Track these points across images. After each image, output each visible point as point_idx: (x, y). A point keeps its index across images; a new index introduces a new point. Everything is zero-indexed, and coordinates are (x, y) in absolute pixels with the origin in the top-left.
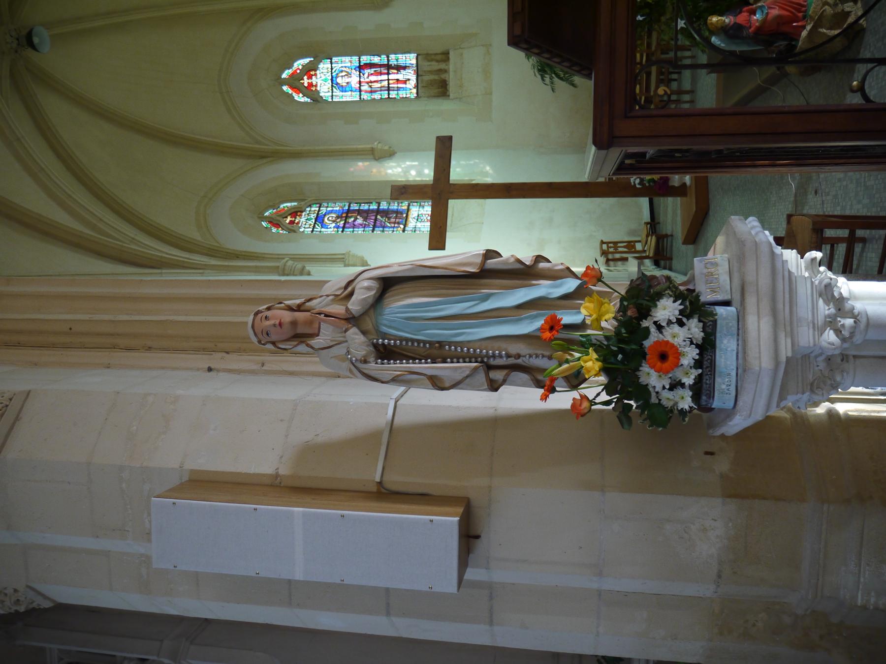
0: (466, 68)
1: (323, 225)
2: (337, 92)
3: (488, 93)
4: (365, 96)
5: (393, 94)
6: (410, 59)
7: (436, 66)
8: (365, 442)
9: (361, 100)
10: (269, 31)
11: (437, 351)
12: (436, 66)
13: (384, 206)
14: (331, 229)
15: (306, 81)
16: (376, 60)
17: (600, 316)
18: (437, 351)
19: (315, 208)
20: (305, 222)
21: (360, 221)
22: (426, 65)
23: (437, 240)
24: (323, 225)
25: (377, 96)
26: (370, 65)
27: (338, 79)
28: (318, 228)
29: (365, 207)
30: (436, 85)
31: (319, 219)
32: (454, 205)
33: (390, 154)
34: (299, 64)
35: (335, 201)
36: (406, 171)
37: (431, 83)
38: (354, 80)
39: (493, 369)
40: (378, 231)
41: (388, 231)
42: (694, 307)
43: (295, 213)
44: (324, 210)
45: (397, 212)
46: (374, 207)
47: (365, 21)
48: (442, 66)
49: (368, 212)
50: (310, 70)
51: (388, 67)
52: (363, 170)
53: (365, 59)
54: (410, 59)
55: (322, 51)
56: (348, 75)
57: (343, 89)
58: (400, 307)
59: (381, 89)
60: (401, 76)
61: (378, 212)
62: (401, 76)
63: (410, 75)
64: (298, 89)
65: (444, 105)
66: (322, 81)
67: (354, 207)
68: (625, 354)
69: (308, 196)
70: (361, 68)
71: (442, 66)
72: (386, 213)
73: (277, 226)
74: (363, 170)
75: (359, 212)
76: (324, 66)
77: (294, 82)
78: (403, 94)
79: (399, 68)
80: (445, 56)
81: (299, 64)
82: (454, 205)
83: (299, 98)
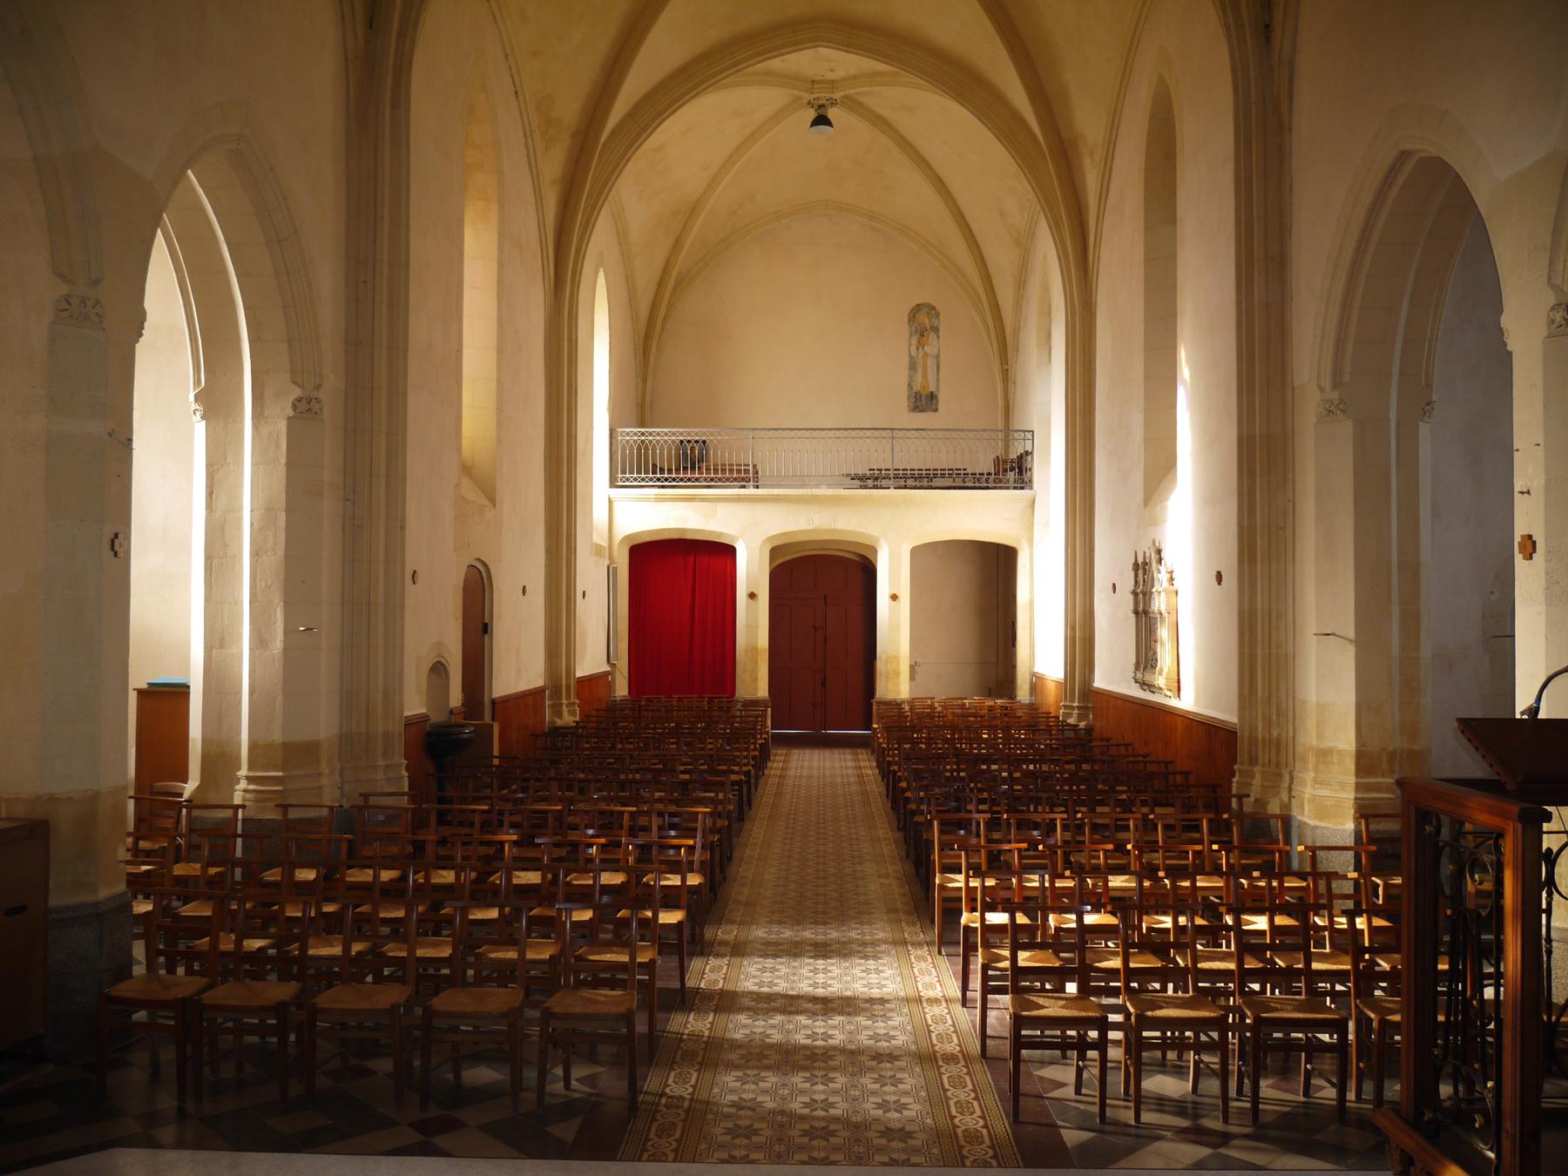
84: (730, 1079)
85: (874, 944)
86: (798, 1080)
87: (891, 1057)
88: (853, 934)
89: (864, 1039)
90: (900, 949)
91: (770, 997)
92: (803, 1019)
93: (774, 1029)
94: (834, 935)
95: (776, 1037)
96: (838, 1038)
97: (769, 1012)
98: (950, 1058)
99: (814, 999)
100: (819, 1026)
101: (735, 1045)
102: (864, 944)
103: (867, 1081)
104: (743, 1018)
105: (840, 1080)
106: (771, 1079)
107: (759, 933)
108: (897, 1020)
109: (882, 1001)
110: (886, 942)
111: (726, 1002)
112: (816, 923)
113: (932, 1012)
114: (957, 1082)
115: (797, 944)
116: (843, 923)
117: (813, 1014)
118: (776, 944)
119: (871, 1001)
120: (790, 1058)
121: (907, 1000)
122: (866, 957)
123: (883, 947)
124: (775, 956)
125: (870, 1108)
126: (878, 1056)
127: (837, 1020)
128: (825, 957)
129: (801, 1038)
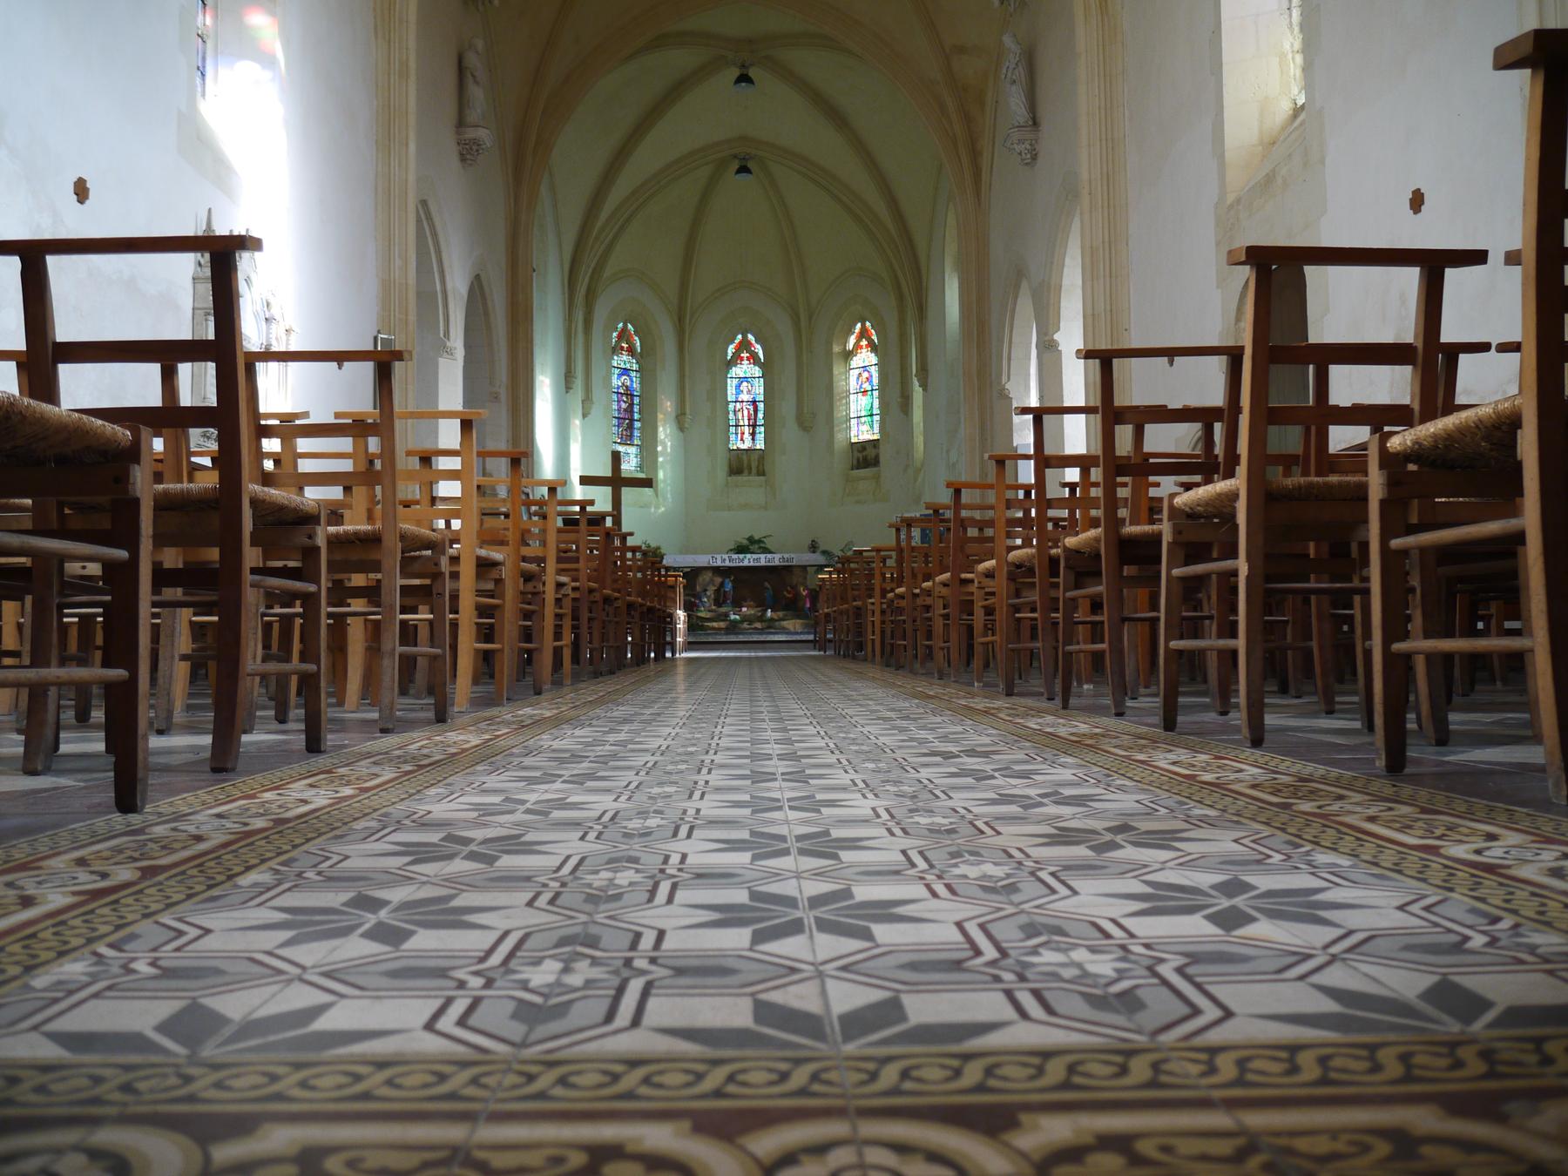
0: (751, 489)
1: (620, 375)
2: (735, 382)
3: (729, 509)
4: (731, 406)
5: (732, 429)
6: (760, 445)
9: (728, 403)
10: (784, 327)
13: (637, 425)
14: (616, 382)
15: (745, 355)
16: (760, 415)
19: (635, 367)
20: (622, 360)
21: (624, 406)
22: (754, 457)
24: (620, 375)
25: (731, 416)
26: (756, 411)
27: (745, 383)
29: (636, 408)
30: (740, 464)
31: (625, 371)
32: (608, 490)
33: (681, 428)
37: (740, 461)
38: (745, 397)
40: (615, 422)
41: (615, 429)
43: (631, 351)
45: (631, 437)
46: (636, 416)
47: (788, 408)
48: (754, 470)
49: (632, 412)
50: (754, 358)
51: (755, 426)
52: (667, 406)
53: (761, 406)
54: (760, 445)
55: (767, 368)
57: (738, 386)
60: (747, 436)
61: (632, 420)
62: (747, 436)
63: (747, 444)
64: (739, 349)
65: (721, 472)
66: (744, 369)
67: (636, 400)
69: (647, 361)
70: (754, 402)
71: (754, 470)
72: (631, 427)
73: (620, 337)
74: (667, 406)
75: (632, 405)
76: (757, 371)
77: (746, 345)
78: (733, 437)
79: (753, 434)
80: (761, 473)
82: (608, 490)
83: (731, 349)
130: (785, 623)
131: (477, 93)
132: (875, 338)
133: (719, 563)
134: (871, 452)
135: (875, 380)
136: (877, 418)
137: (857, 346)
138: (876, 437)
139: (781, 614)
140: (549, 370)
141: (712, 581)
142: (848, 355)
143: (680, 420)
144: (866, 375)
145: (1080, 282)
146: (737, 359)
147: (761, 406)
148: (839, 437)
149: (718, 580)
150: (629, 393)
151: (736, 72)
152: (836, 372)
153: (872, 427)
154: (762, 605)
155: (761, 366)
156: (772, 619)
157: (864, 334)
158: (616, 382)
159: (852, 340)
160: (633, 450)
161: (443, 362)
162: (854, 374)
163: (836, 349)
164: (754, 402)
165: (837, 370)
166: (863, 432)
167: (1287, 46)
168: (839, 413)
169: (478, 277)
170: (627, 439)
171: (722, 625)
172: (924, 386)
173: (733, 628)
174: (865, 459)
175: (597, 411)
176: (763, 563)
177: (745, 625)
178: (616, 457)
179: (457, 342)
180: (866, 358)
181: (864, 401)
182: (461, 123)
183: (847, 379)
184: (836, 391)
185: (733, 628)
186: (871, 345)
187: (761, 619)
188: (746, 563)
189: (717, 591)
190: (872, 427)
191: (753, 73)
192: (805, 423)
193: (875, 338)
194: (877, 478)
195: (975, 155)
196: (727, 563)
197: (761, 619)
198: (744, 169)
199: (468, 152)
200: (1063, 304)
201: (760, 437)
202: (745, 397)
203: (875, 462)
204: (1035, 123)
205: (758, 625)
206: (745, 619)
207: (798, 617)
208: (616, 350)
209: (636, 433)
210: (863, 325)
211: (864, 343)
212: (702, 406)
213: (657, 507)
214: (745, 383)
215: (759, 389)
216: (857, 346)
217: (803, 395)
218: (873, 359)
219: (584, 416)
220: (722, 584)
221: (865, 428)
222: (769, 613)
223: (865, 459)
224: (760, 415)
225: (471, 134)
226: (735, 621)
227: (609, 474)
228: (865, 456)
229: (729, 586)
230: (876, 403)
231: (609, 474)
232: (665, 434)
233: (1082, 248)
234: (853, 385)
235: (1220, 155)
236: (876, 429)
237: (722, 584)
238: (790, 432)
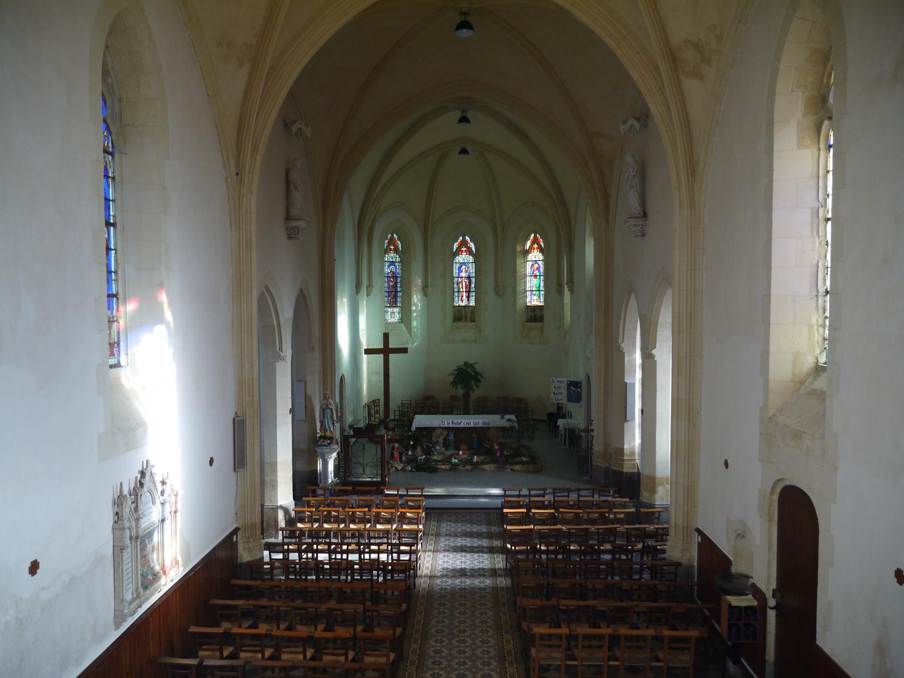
0: (466, 331)
1: (389, 266)
2: (458, 266)
4: (456, 280)
5: (456, 294)
6: (472, 303)
7: (469, 315)
8: (311, 404)
9: (453, 278)
11: (324, 416)
12: (469, 315)
13: (400, 294)
14: (387, 270)
15: (464, 249)
16: (473, 285)
17: (328, 434)
18: (324, 416)
19: (398, 259)
20: (391, 256)
21: (391, 284)
22: (469, 311)
23: (367, 352)
26: (470, 283)
27: (464, 264)
28: (387, 264)
30: (461, 315)
31: (392, 263)
32: (381, 357)
34: (472, 246)
35: (402, 269)
36: (416, 305)
39: (322, 422)
40: (386, 294)
41: (386, 299)
42: (329, 444)
43: (396, 250)
44: (397, 264)
45: (396, 302)
46: (399, 289)
47: (489, 282)
48: (468, 319)
50: (469, 251)
52: (418, 281)
53: (473, 280)
54: (472, 303)
55: (477, 257)
56: (466, 271)
57: (460, 268)
58: (329, 411)
59: (459, 288)
60: (464, 298)
61: (396, 292)
62: (464, 298)
64: (460, 246)
66: (463, 258)
67: (399, 280)
68: (324, 437)
69: (404, 254)
70: (469, 278)
71: (468, 319)
72: (395, 296)
73: (389, 243)
75: (396, 283)
76: (471, 259)
77: (464, 243)
78: (456, 299)
79: (468, 297)
80: (473, 320)
81: (472, 246)
82: (381, 357)
83: (456, 246)
84: (484, 530)
85: (443, 576)
86: (469, 530)
87: (446, 535)
88: (450, 581)
89: (452, 539)
90: (433, 574)
91: (478, 552)
92: (469, 545)
93: (476, 542)
94: (457, 581)
95: (475, 540)
96: (459, 540)
97: (478, 547)
98: (432, 535)
99: (465, 551)
100: (464, 543)
101: (485, 538)
102: (446, 576)
103: (453, 530)
104: (485, 545)
105: (459, 530)
106: (475, 530)
107: (488, 582)
108: (442, 545)
109: (445, 551)
110: (437, 577)
111: (491, 550)
112: (465, 589)
113: (432, 548)
114: (433, 530)
115: (472, 576)
116: (453, 589)
117: (465, 546)
118: (480, 576)
119: (448, 551)
120: (471, 535)
121: (437, 551)
122: (447, 569)
123: (439, 574)
124: (479, 569)
125: (453, 525)
126: (450, 535)
127: (459, 545)
128: (461, 569)
129: (469, 539)
130: (486, 467)
131: (297, 196)
132: (542, 244)
133: (446, 425)
134: (539, 313)
135: (542, 270)
136: (542, 293)
137: (531, 247)
138: (542, 304)
139: (482, 458)
140: (345, 300)
141: (442, 434)
142: (526, 253)
143: (425, 289)
144: (536, 266)
145: (670, 320)
146: (459, 252)
147: (473, 280)
148: (520, 302)
149: (446, 432)
150: (394, 276)
151: (458, 115)
152: (518, 262)
153: (539, 297)
154: (475, 449)
155: (473, 255)
156: (477, 463)
157: (536, 241)
158: (387, 270)
159: (528, 244)
160: (396, 310)
161: (279, 365)
162: (529, 264)
163: (519, 248)
164: (469, 278)
165: (519, 261)
166: (535, 300)
167: (814, 321)
168: (520, 288)
169: (301, 290)
170: (393, 304)
171: (447, 467)
172: (571, 291)
173: (454, 468)
174: (535, 316)
175: (375, 291)
176: (472, 425)
177: (461, 467)
178: (386, 336)
179: (288, 352)
180: (536, 256)
181: (535, 282)
182: (288, 218)
183: (525, 267)
184: (518, 274)
185: (454, 468)
186: (540, 247)
187: (470, 462)
188: (462, 425)
189: (445, 439)
190: (539, 297)
191: (469, 115)
192: (499, 291)
193: (542, 244)
194: (542, 329)
195: (606, 196)
196: (451, 425)
197: (470, 462)
198: (464, 151)
199: (292, 234)
200: (658, 333)
201: (473, 299)
202: (463, 274)
203: (540, 319)
204: (645, 216)
205: (469, 467)
206: (464, 462)
207: (494, 463)
208: (387, 251)
209: (399, 300)
210: (535, 236)
211: (536, 246)
212: (438, 280)
213: (412, 343)
214: (464, 264)
215: (472, 270)
216: (531, 247)
217: (499, 275)
218: (541, 257)
219: (368, 295)
220: (448, 435)
221: (535, 298)
222: (475, 459)
223: (535, 316)
224: (473, 285)
225: (293, 224)
226: (455, 465)
227: (382, 347)
228: (535, 315)
229: (451, 437)
230: (542, 284)
231: (382, 347)
232: (417, 299)
233: (673, 312)
234: (528, 270)
235: (766, 381)
236: (542, 300)
237: (448, 435)
238: (490, 297)
